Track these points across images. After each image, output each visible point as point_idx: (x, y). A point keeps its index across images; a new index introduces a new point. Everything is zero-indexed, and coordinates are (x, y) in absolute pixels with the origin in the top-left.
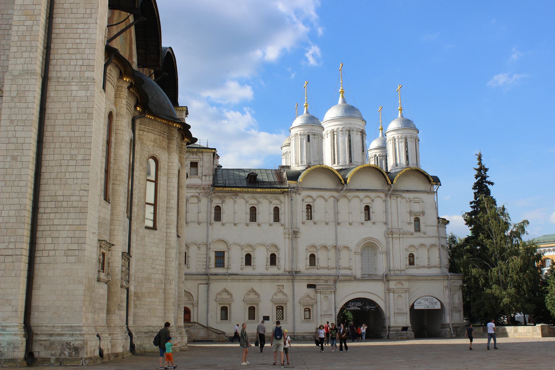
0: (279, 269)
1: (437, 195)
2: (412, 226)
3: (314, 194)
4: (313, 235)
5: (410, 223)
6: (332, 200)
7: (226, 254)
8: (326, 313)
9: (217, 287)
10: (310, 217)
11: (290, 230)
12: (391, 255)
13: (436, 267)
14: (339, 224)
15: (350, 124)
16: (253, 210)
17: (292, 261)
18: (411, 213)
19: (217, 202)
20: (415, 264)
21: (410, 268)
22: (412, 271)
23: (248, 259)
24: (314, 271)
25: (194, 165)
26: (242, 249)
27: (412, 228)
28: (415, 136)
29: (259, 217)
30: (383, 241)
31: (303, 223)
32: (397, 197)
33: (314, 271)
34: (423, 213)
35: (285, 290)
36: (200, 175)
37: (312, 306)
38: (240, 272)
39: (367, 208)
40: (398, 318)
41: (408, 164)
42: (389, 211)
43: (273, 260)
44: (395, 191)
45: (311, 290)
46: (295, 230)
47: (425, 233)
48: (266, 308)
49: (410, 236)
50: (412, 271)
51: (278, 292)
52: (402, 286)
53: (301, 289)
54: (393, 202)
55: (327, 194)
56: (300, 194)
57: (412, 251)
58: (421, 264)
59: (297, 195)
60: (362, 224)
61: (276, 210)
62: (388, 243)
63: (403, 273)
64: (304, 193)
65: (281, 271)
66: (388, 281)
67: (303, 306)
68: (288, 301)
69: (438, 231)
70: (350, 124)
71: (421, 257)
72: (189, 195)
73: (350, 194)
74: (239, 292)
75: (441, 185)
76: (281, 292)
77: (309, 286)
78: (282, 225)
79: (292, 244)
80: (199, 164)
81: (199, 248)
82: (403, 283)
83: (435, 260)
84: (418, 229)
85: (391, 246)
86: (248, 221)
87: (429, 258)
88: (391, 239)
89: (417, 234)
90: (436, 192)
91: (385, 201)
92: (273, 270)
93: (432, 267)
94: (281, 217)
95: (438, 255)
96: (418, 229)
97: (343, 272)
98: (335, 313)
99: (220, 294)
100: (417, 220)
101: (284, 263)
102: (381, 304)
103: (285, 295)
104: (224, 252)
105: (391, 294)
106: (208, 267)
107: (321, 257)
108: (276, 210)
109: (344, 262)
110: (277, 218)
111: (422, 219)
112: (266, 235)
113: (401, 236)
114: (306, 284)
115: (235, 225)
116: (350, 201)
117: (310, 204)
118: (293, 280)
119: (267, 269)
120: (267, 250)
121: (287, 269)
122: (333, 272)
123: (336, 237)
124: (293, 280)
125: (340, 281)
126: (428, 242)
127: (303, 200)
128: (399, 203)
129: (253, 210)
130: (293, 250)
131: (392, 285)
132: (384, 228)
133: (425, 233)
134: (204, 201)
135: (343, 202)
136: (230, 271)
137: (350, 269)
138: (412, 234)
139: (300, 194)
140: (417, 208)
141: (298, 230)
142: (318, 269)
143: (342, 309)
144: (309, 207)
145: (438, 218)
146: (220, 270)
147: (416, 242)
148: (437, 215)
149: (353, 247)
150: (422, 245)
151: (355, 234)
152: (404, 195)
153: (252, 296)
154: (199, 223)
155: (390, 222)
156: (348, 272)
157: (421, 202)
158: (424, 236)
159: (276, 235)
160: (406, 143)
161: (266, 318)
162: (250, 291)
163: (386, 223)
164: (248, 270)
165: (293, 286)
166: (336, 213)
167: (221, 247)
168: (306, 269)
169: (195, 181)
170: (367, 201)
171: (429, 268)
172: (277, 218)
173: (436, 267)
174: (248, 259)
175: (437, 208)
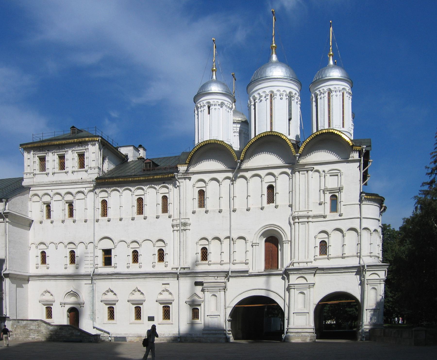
7: (113, 251)
11: (178, 221)
16: (140, 201)
23: (136, 256)
25: (81, 156)
29: (146, 209)
30: (287, 228)
31: (194, 212)
43: (161, 256)
45: (199, 288)
46: (183, 221)
49: (322, 219)
51: (164, 291)
52: (304, 281)
56: (190, 179)
59: (187, 180)
64: (195, 178)
65: (168, 270)
68: (173, 300)
73: (248, 175)
80: (86, 155)
89: (331, 216)
91: (291, 178)
93: (348, 257)
103: (170, 293)
107: (214, 249)
109: (239, 257)
110: (165, 210)
129: (140, 201)
131: (294, 279)
139: (190, 179)
141: (187, 221)
142: (209, 264)
144: (202, 193)
147: (329, 227)
153: (137, 296)
154: (86, 221)
156: (243, 267)
163: (291, 206)
166: (232, 198)
167: (107, 245)
171: (343, 258)
172: (165, 210)
174: (136, 256)
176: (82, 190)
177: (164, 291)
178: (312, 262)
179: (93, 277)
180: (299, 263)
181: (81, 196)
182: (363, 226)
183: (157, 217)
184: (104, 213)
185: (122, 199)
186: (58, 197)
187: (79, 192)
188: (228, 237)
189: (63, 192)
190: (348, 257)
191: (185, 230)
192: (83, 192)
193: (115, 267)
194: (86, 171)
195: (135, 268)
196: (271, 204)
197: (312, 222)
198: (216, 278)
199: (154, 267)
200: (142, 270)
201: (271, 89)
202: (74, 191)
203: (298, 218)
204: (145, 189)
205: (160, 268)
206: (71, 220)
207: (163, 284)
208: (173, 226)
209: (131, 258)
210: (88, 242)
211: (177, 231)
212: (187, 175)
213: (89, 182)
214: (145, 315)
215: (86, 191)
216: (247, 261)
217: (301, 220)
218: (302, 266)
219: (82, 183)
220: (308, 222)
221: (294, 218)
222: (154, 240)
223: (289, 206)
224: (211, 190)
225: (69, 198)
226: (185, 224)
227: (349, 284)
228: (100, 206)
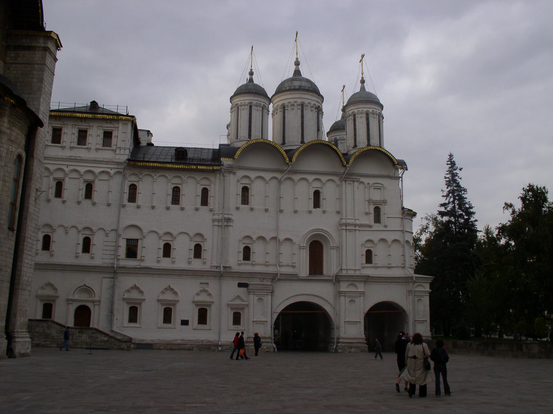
0: (204, 263)
1: (402, 181)
2: (372, 216)
3: (253, 175)
4: (248, 223)
5: (367, 214)
8: (261, 320)
9: (126, 282)
10: (245, 200)
12: (344, 251)
14: (281, 211)
16: (176, 191)
19: (132, 179)
20: (373, 262)
21: (367, 267)
23: (167, 250)
25: (108, 135)
26: (160, 238)
27: (370, 220)
28: (378, 111)
29: (183, 200)
31: (238, 209)
32: (354, 182)
33: (247, 268)
35: (210, 289)
36: (114, 147)
37: (243, 309)
39: (317, 194)
41: (369, 145)
43: (198, 251)
44: (352, 174)
46: (226, 216)
47: (386, 226)
48: (186, 310)
49: (369, 229)
50: (369, 271)
54: (348, 188)
55: (268, 176)
56: (234, 173)
57: (369, 246)
59: (232, 175)
60: (310, 212)
63: (358, 273)
64: (240, 173)
65: (207, 267)
66: (339, 282)
67: (232, 309)
69: (403, 225)
73: (296, 177)
75: (407, 169)
77: (240, 285)
78: (211, 210)
82: (357, 284)
84: (377, 220)
85: (344, 240)
86: (170, 205)
88: (344, 232)
89: (376, 226)
90: (402, 177)
92: (197, 265)
94: (210, 200)
96: (377, 220)
98: (272, 318)
99: (128, 291)
100: (377, 211)
101: (210, 258)
102: (328, 309)
103: (210, 295)
104: (137, 240)
107: (257, 250)
108: (205, 192)
109: (285, 259)
110: (205, 201)
112: (189, 221)
113: (357, 228)
114: (237, 282)
117: (247, 186)
119: (189, 263)
120: (191, 239)
121: (215, 264)
123: (277, 226)
125: (279, 280)
126: (390, 237)
127: (238, 181)
128: (356, 189)
129: (176, 191)
131: (344, 287)
134: (118, 179)
135: (286, 187)
136: (143, 264)
137: (294, 267)
138: (370, 226)
139: (234, 173)
140: (376, 196)
141: (230, 216)
142: (253, 265)
144: (245, 190)
145: (403, 208)
146: (131, 263)
147: (376, 237)
148: (402, 205)
150: (383, 240)
151: (301, 225)
152: (362, 179)
153: (169, 296)
154: (109, 205)
155: (344, 211)
157: (382, 188)
158: (385, 229)
160: (368, 119)
161: (185, 323)
162: (166, 289)
163: (338, 212)
164: (166, 263)
167: (133, 234)
168: (239, 265)
169: (106, 155)
170: (317, 185)
172: (205, 201)
174: (167, 250)
175: (401, 196)
176: (108, 170)
177: (201, 291)
178: (359, 270)
180: (347, 270)
181: (105, 177)
182: (406, 239)
186: (75, 175)
187: (103, 172)
188: (274, 238)
189: (82, 170)
190: (393, 267)
191: (227, 226)
192: (108, 173)
193: (142, 261)
194: (113, 150)
195: (166, 263)
196: (318, 209)
197: (359, 230)
198: (262, 280)
199: (189, 263)
200: (175, 266)
201: (304, 100)
202: (97, 171)
203: (346, 225)
204: (184, 179)
205: (197, 265)
206: (88, 202)
207: (201, 283)
208: (214, 221)
209: (161, 252)
210: (109, 229)
211: (218, 226)
212: (231, 170)
213: (118, 163)
214: (178, 316)
215: (112, 172)
216: (294, 264)
217: (348, 228)
218: (351, 273)
219: (108, 162)
220: (355, 230)
221: (341, 225)
222: (192, 234)
224: (257, 189)
225: (89, 177)
226: (229, 220)
227: (394, 295)
228: (127, 190)
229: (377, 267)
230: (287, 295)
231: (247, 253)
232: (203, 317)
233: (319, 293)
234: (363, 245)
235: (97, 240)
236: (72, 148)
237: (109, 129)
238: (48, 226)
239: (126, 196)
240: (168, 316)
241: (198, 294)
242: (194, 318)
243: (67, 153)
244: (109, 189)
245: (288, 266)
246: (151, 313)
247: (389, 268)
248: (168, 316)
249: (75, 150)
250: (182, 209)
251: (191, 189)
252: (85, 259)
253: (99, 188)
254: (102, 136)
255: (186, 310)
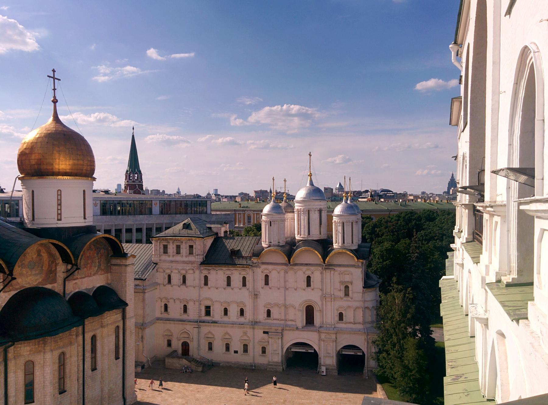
0: (246, 319)
3: (270, 267)
4: (269, 296)
5: (340, 290)
6: (282, 273)
9: (205, 329)
10: (267, 283)
13: (359, 323)
15: (309, 205)
16: (229, 278)
17: (254, 314)
18: (341, 282)
22: (341, 325)
23: (226, 312)
24: (269, 321)
27: (342, 294)
30: (320, 303)
31: (262, 288)
34: (351, 283)
36: (194, 255)
38: (220, 320)
39: (309, 278)
40: (328, 359)
42: (324, 280)
43: (242, 312)
45: (266, 335)
48: (236, 345)
53: (259, 334)
54: (328, 274)
55: (279, 268)
58: (348, 321)
60: (304, 290)
61: (244, 279)
62: (322, 304)
64: (263, 267)
65: (247, 321)
70: (309, 205)
71: (349, 316)
72: (188, 268)
73: (296, 268)
74: (218, 333)
76: (246, 335)
77: (264, 332)
78: (248, 289)
79: (254, 303)
80: (194, 247)
81: (194, 304)
83: (360, 319)
84: (347, 294)
87: (354, 317)
91: (321, 273)
92: (242, 320)
95: (362, 315)
96: (347, 294)
97: (289, 323)
100: (347, 287)
105: (322, 342)
106: (200, 317)
108: (244, 279)
110: (244, 285)
111: (350, 286)
115: (217, 288)
116: (295, 273)
118: (254, 328)
119: (238, 319)
120: (238, 306)
122: (283, 322)
124: (254, 328)
125: (286, 330)
127: (262, 272)
129: (229, 278)
130: (255, 307)
132: (320, 293)
133: (352, 298)
134: (197, 272)
135: (291, 274)
136: (214, 319)
139: (260, 267)
143: (288, 349)
144: (267, 277)
146: (208, 318)
149: (297, 306)
150: (349, 307)
151: (300, 297)
153: (227, 337)
154: (194, 287)
159: (243, 296)
161: (236, 352)
164: (226, 319)
165: (254, 332)
167: (208, 303)
169: (191, 258)
170: (308, 273)
172: (244, 285)
173: (359, 323)
174: (226, 312)
179: (199, 322)
183: (240, 289)
184: (206, 284)
185: (218, 275)
214: (232, 349)
223: (321, 290)
226: (256, 295)
228: (203, 279)
229: (346, 323)
230: (292, 338)
231: (269, 313)
232: (245, 349)
233: (310, 337)
234: (338, 310)
235: (190, 306)
236: (173, 256)
237: (191, 244)
238: (166, 299)
239: (203, 282)
240: (228, 348)
241: (242, 337)
242: (240, 349)
243: (171, 258)
244: (195, 277)
245: (291, 320)
246: (219, 347)
247: (355, 323)
248: (228, 348)
249: (175, 257)
250: (232, 289)
251: (236, 276)
252: (185, 317)
253: (189, 278)
254: (188, 248)
255: (236, 345)
